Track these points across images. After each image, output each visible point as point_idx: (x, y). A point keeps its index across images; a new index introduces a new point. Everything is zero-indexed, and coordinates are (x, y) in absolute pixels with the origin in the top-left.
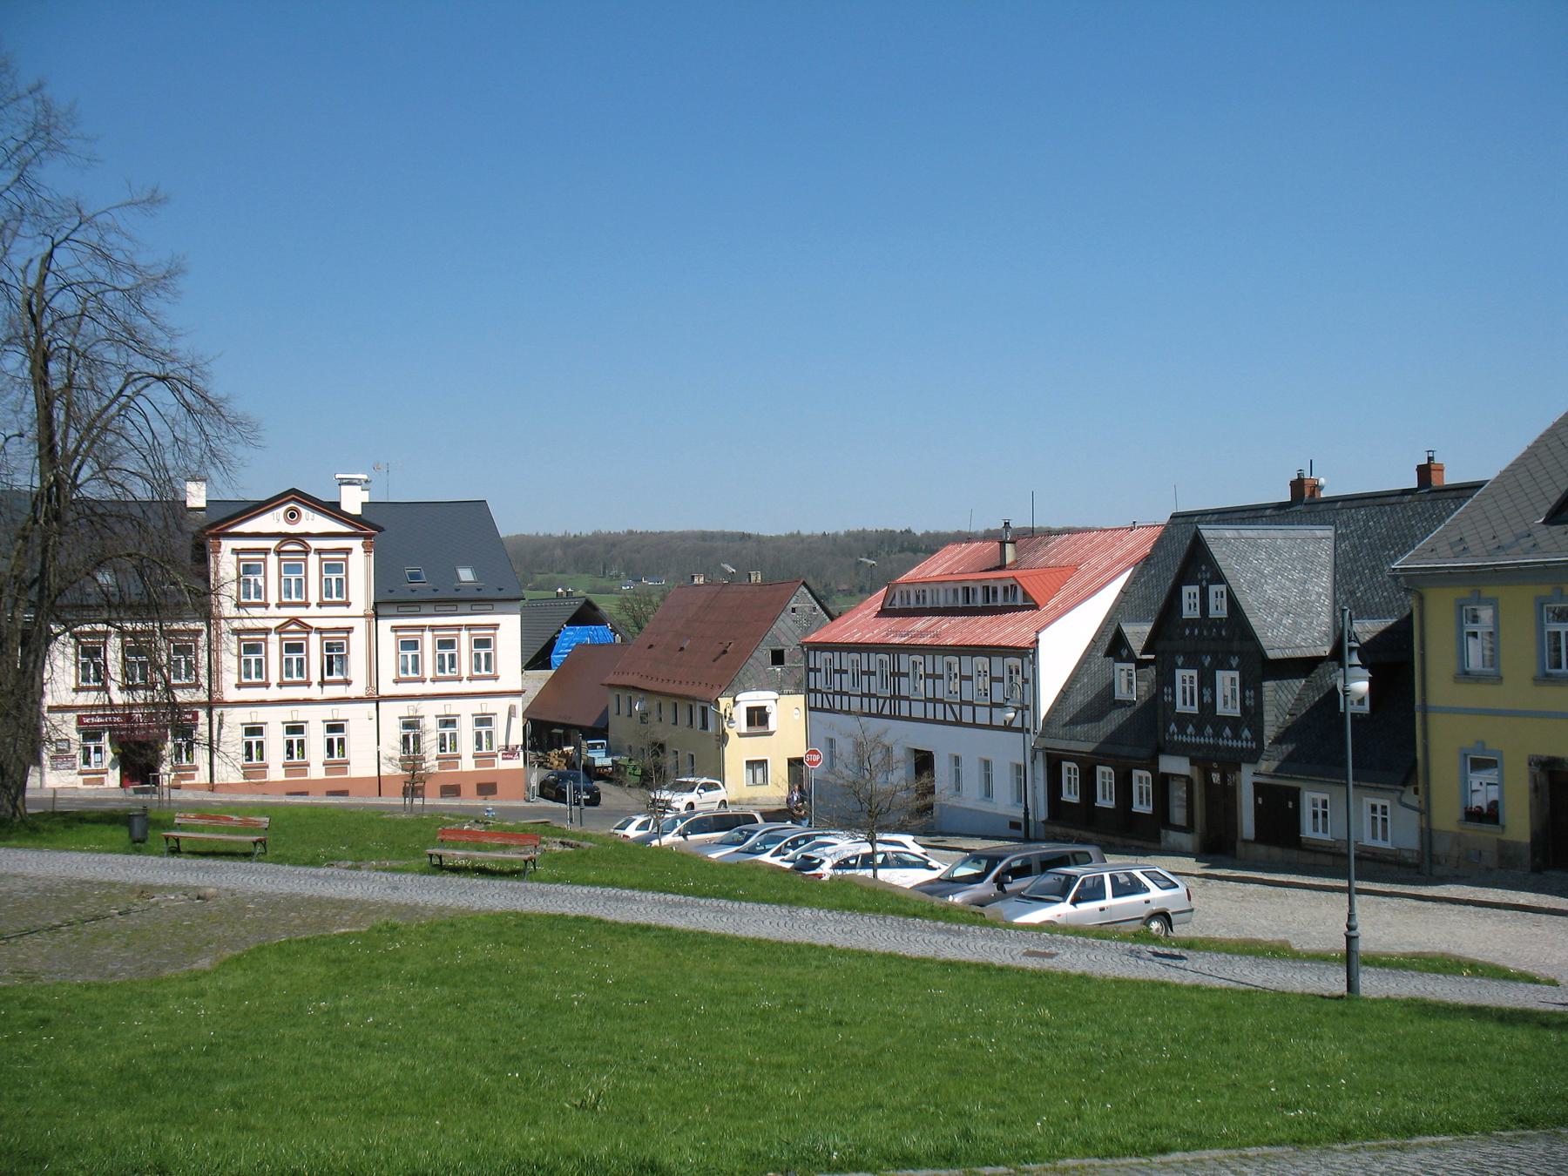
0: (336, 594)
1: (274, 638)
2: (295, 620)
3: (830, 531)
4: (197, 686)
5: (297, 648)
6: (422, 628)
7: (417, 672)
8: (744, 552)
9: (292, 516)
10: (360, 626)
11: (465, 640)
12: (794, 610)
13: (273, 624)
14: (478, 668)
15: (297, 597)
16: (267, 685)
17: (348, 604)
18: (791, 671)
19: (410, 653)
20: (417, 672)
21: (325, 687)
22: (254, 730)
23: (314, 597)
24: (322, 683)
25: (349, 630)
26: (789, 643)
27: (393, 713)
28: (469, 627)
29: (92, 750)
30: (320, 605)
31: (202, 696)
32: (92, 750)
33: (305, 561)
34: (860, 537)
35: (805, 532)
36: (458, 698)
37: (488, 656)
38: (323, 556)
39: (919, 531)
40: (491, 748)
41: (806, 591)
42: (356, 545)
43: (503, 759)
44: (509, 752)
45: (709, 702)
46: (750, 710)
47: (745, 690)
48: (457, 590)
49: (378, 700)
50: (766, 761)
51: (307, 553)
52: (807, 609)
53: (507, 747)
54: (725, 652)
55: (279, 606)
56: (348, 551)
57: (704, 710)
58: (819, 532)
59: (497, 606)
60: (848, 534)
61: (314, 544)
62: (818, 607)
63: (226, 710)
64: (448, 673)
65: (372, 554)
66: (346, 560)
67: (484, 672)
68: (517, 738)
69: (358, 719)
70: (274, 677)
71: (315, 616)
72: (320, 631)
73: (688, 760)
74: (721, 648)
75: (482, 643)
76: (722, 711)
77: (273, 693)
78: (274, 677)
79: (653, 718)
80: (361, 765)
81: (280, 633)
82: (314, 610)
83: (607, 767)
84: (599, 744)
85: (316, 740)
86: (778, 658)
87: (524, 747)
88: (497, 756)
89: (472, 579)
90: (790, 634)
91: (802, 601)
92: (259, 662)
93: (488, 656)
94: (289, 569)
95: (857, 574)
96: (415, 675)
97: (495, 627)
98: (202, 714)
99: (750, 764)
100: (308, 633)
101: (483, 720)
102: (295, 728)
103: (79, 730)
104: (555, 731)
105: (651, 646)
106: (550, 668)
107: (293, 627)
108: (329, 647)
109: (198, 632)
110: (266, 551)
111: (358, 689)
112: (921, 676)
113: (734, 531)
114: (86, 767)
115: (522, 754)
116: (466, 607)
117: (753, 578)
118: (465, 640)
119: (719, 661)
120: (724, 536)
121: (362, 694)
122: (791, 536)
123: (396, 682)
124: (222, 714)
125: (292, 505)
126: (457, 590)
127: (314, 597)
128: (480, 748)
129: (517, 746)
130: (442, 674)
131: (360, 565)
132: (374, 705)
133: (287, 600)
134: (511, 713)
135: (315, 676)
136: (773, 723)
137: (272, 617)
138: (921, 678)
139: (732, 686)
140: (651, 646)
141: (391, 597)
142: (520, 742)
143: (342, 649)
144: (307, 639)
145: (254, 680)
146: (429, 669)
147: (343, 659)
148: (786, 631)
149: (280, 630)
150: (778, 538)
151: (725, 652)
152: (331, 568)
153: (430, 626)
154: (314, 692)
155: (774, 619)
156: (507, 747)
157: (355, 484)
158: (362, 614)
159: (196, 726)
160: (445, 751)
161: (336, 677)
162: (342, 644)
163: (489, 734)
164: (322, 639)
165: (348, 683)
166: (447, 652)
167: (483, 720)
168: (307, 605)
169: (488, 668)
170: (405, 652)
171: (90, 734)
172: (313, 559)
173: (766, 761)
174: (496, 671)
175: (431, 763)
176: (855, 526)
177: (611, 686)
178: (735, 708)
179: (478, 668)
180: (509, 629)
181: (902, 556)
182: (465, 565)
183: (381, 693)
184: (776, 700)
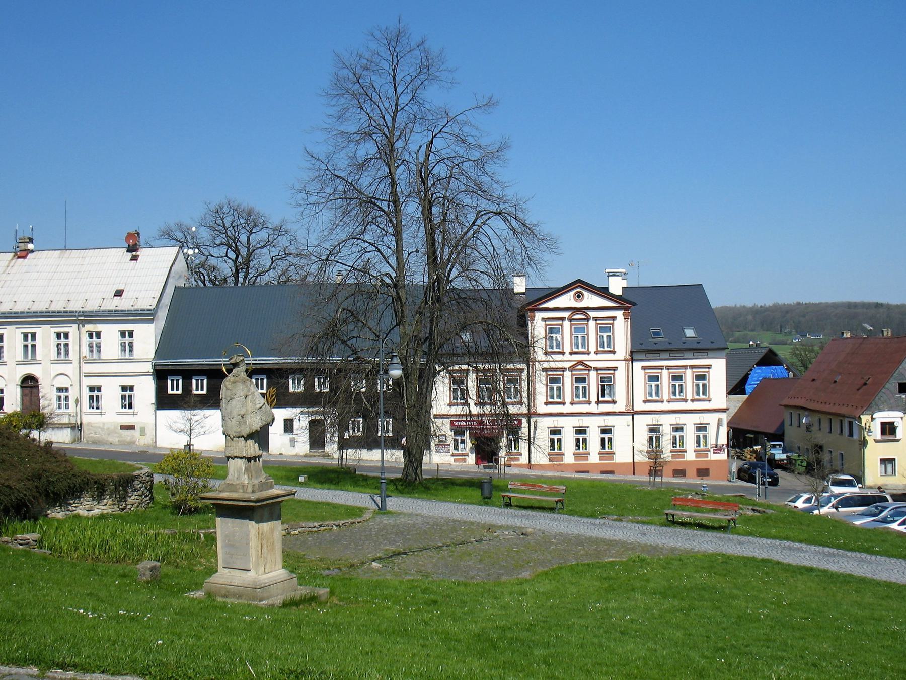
0: (606, 345)
1: (568, 374)
2: (581, 362)
4: (521, 403)
5: (583, 380)
6: (661, 368)
7: (658, 396)
10: (622, 366)
11: (689, 375)
13: (567, 365)
14: (698, 394)
15: (582, 347)
16: (564, 404)
17: (614, 352)
19: (653, 384)
20: (658, 396)
21: (600, 405)
22: (555, 431)
23: (593, 348)
24: (598, 402)
25: (615, 369)
27: (643, 422)
28: (692, 367)
29: (459, 441)
30: (596, 353)
31: (524, 410)
32: (459, 441)
33: (587, 325)
36: (685, 413)
37: (704, 386)
38: (598, 322)
40: (706, 446)
42: (619, 314)
43: (714, 453)
44: (718, 449)
45: (854, 418)
46: (883, 425)
47: (880, 410)
48: (684, 343)
49: (633, 413)
50: (894, 460)
51: (588, 320)
53: (716, 445)
54: (865, 384)
55: (571, 353)
56: (614, 318)
57: (851, 424)
59: (710, 353)
61: (592, 314)
63: (539, 419)
64: (678, 397)
65: (629, 320)
66: (613, 324)
67: (702, 396)
68: (723, 440)
69: (620, 424)
70: (568, 398)
71: (593, 360)
72: (596, 369)
73: (839, 457)
74: (863, 381)
76: (863, 424)
77: (568, 408)
78: (568, 398)
79: (815, 428)
80: (622, 454)
81: (572, 371)
82: (593, 356)
85: (594, 438)
87: (728, 446)
88: (710, 451)
89: (694, 336)
92: (559, 389)
93: (704, 386)
94: (578, 330)
96: (657, 398)
97: (709, 367)
98: (524, 420)
99: (883, 461)
100: (589, 370)
101: (701, 428)
102: (581, 431)
103: (451, 429)
104: (748, 435)
105: (814, 380)
106: (744, 394)
107: (580, 367)
108: (602, 380)
109: (522, 370)
110: (562, 319)
111: (621, 406)
114: (456, 452)
115: (726, 450)
116: (690, 354)
117: (885, 334)
118: (689, 375)
119: (861, 391)
121: (623, 410)
123: (645, 402)
124: (536, 421)
126: (684, 343)
127: (593, 348)
128: (699, 446)
129: (723, 445)
130: (674, 398)
131: (621, 327)
132: (631, 417)
133: (576, 350)
135: (594, 398)
136: (899, 434)
137: (566, 360)
139: (870, 407)
140: (814, 380)
142: (725, 442)
143: (610, 381)
144: (588, 375)
145: (556, 400)
146: (666, 394)
147: (611, 387)
149: (572, 368)
151: (865, 384)
152: (603, 329)
153: (666, 366)
154: (593, 408)
156: (716, 445)
158: (623, 359)
159: (520, 428)
160: (676, 447)
161: (607, 398)
162: (611, 377)
163: (705, 437)
164: (598, 375)
165: (614, 402)
166: (677, 383)
167: (701, 428)
168: (588, 353)
169: (704, 394)
171: (458, 432)
172: (592, 324)
173: (894, 460)
175: (667, 453)
178: (873, 422)
179: (698, 394)
182: (689, 326)
183: (635, 409)
184: (902, 418)
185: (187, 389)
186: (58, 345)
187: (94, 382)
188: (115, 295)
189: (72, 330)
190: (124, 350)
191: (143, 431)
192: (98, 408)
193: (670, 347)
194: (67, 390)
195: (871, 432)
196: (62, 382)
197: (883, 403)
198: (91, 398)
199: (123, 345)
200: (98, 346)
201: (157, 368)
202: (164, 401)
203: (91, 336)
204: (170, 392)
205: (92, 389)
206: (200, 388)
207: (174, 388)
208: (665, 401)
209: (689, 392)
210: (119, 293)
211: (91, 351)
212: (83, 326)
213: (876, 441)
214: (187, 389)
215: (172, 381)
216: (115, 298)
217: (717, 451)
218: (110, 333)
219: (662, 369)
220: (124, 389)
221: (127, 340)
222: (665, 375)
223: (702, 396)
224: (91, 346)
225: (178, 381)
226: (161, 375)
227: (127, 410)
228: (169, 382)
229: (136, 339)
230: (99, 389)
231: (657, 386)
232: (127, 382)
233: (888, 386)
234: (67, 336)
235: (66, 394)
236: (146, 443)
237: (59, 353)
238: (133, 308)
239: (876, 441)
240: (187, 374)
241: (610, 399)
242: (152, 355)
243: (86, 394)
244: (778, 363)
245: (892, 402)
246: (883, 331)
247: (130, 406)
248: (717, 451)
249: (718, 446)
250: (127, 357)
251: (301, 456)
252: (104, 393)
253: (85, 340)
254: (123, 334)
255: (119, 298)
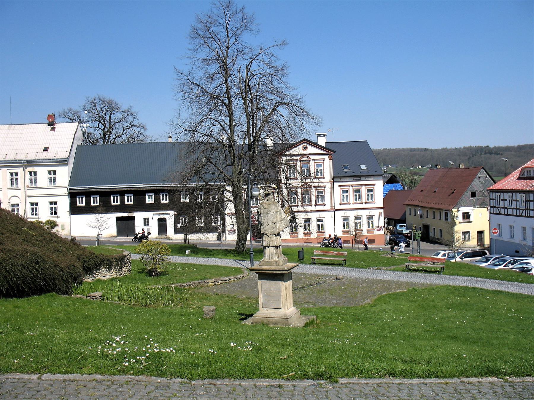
3: (458, 147)
5: (307, 193)
6: (349, 186)
8: (426, 155)
9: (305, 148)
10: (328, 185)
11: (364, 190)
12: (479, 177)
14: (368, 199)
18: (478, 199)
24: (316, 205)
25: (325, 187)
26: (477, 189)
27: (339, 215)
28: (365, 185)
34: (470, 149)
35: (449, 147)
36: (362, 210)
37: (371, 195)
39: (492, 146)
40: (373, 227)
41: (484, 171)
42: (326, 157)
45: (449, 211)
46: (464, 214)
47: (462, 206)
48: (361, 172)
50: (469, 232)
51: (310, 161)
52: (484, 177)
54: (453, 193)
57: (446, 214)
58: (454, 147)
59: (375, 178)
60: (465, 148)
61: (312, 157)
62: (488, 176)
64: (358, 201)
65: (332, 160)
66: (323, 163)
67: (370, 201)
68: (382, 224)
69: (328, 217)
72: (315, 187)
73: (439, 231)
74: (452, 191)
75: (370, 191)
76: (453, 214)
79: (425, 215)
81: (302, 188)
83: (407, 234)
84: (403, 225)
86: (473, 195)
87: (384, 226)
88: (375, 230)
90: (478, 186)
91: (482, 174)
93: (371, 195)
95: (469, 162)
96: (347, 202)
97: (374, 185)
99: (464, 233)
100: (311, 188)
101: (370, 217)
105: (422, 191)
108: (318, 193)
110: (296, 160)
111: (328, 207)
112: (524, 201)
113: (422, 148)
115: (383, 229)
117: (461, 166)
118: (364, 190)
119: (451, 196)
120: (418, 150)
121: (329, 208)
122: (444, 149)
123: (340, 204)
125: (304, 144)
126: (361, 172)
128: (369, 227)
129: (382, 226)
131: (328, 164)
132: (333, 212)
134: (380, 215)
138: (524, 202)
139: (457, 204)
140: (422, 191)
141: (339, 175)
142: (383, 225)
143: (322, 194)
146: (351, 199)
147: (323, 197)
148: (477, 185)
150: (439, 150)
151: (453, 193)
153: (352, 185)
154: (313, 208)
155: (472, 181)
156: (378, 227)
157: (323, 136)
161: (320, 203)
163: (372, 222)
165: (324, 205)
166: (357, 194)
167: (370, 217)
169: (371, 199)
170: (343, 194)
172: (312, 163)
173: (469, 232)
174: (374, 200)
176: (467, 145)
177: (407, 205)
178: (458, 213)
179: (368, 199)
180: (379, 186)
181: (486, 155)
183: (335, 208)
184: (473, 210)
185: (88, 202)
186: (11, 179)
187: (34, 200)
188: (44, 151)
189: (20, 171)
190: (50, 181)
191: (63, 227)
192: (36, 215)
193: (354, 174)
194: (18, 205)
195: (458, 218)
196: (15, 201)
197: (463, 203)
198: (32, 209)
199: (50, 179)
200: (36, 180)
201: (71, 191)
202: (75, 210)
203: (31, 174)
204: (78, 204)
205: (32, 204)
206: (95, 202)
207: (81, 202)
208: (351, 204)
209: (364, 198)
210: (46, 149)
211: (31, 183)
212: (26, 169)
213: (460, 223)
214: (88, 202)
215: (79, 198)
216: (44, 152)
217: (379, 230)
218: (42, 172)
219: (349, 186)
220: (51, 203)
221: (52, 176)
222: (351, 190)
223: (370, 201)
224: (31, 180)
225: (82, 198)
226: (73, 195)
227: (53, 215)
228: (78, 199)
229: (57, 175)
230: (37, 204)
231: (347, 196)
232: (53, 199)
233: (466, 193)
234: (16, 174)
235: (18, 207)
236: (65, 233)
237: (12, 184)
238: (55, 158)
239: (460, 223)
240: (88, 194)
241: (322, 203)
242: (67, 184)
243: (29, 207)
244: (398, 182)
245: (468, 202)
246: (459, 165)
247: (56, 213)
248: (379, 230)
249: (379, 227)
250: (53, 185)
251: (154, 238)
252: (39, 207)
253: (28, 176)
254: (50, 173)
255: (46, 152)
